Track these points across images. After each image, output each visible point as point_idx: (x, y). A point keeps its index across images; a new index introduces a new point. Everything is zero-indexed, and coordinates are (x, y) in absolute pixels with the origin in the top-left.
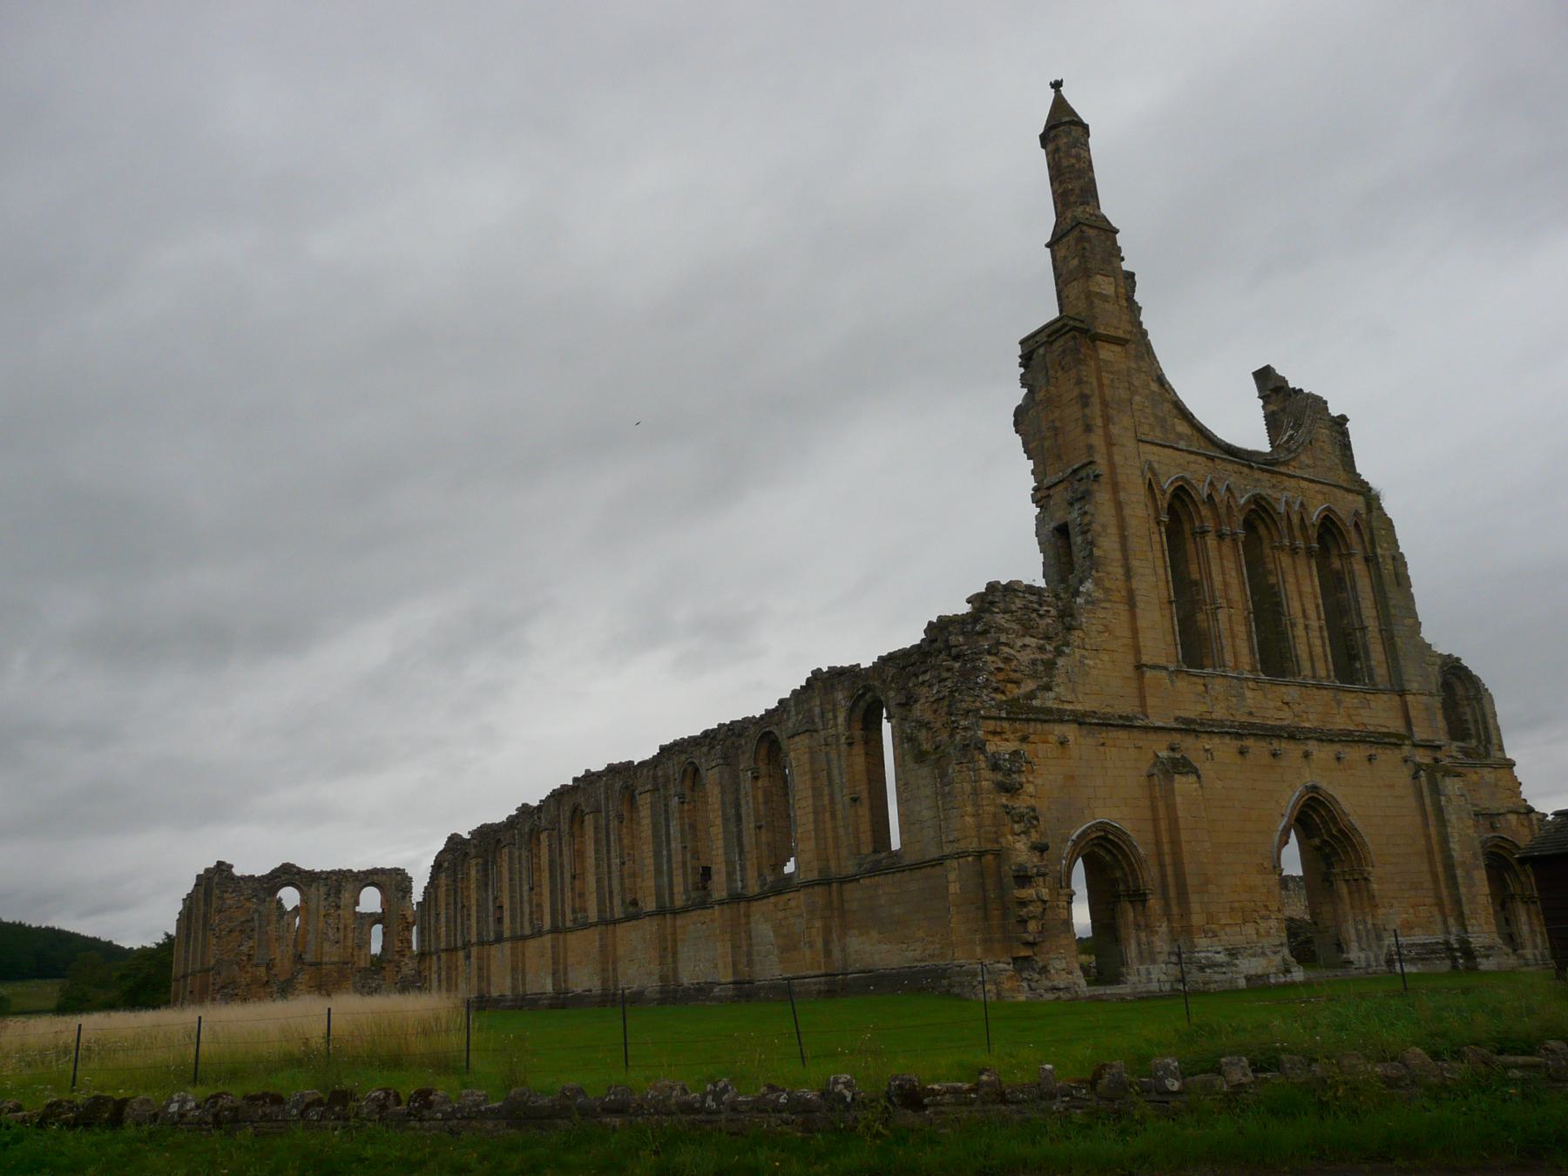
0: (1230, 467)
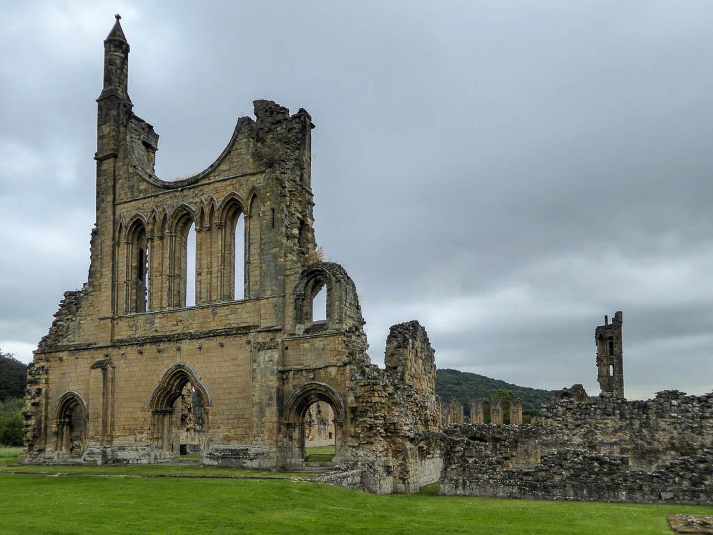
0: (167, 196)
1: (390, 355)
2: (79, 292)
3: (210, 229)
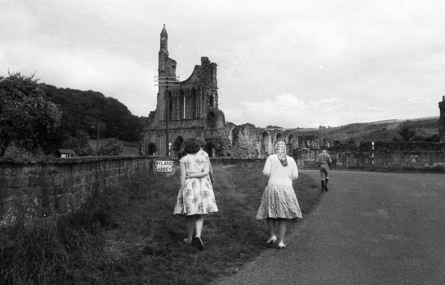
2: (154, 112)
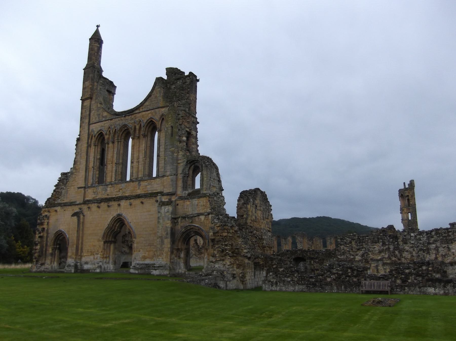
0: (117, 120)
1: (239, 208)
2: (69, 173)
3: (139, 137)
